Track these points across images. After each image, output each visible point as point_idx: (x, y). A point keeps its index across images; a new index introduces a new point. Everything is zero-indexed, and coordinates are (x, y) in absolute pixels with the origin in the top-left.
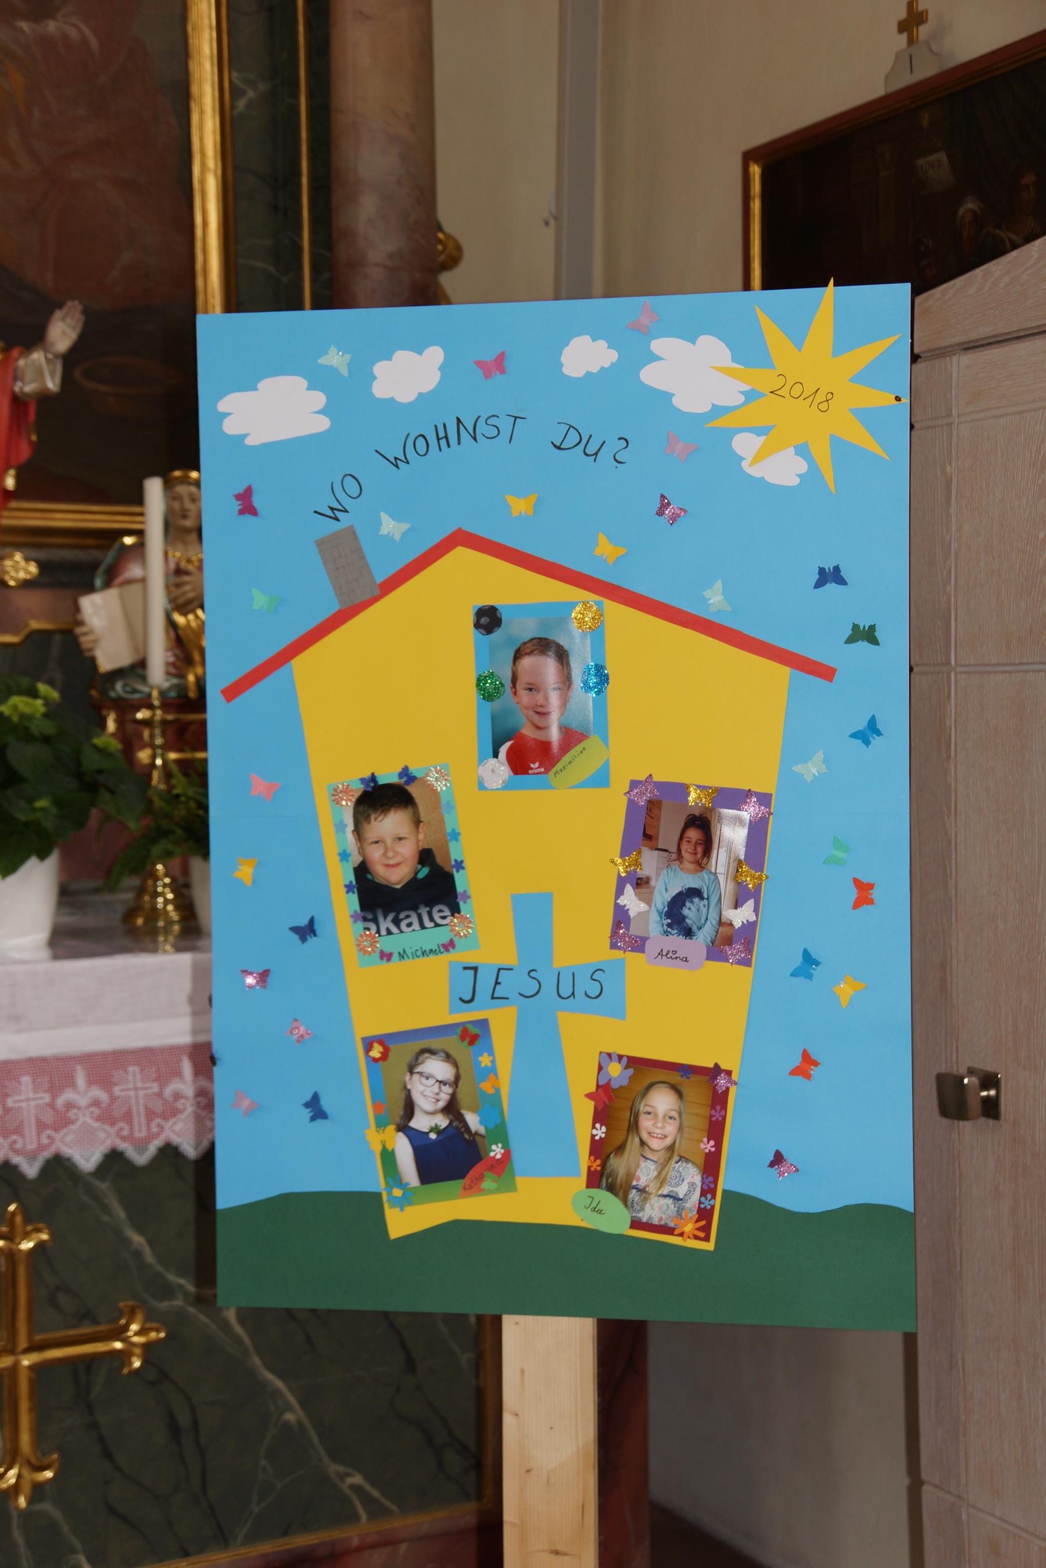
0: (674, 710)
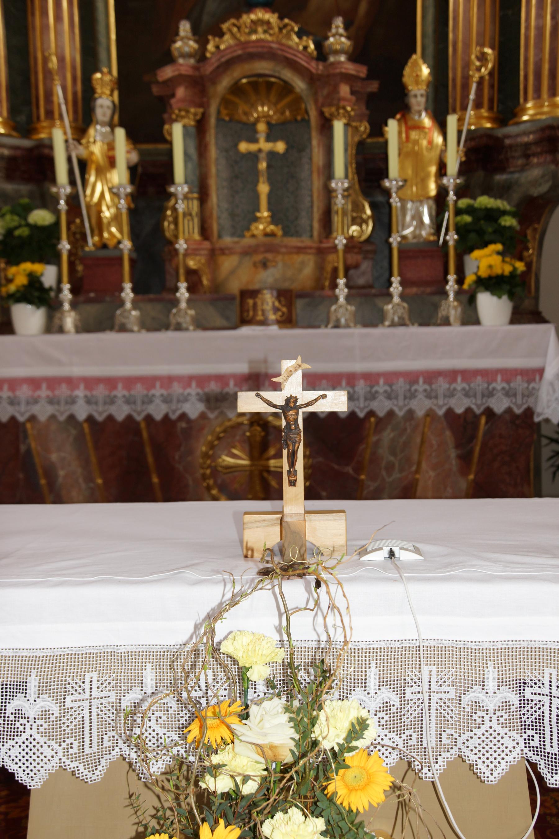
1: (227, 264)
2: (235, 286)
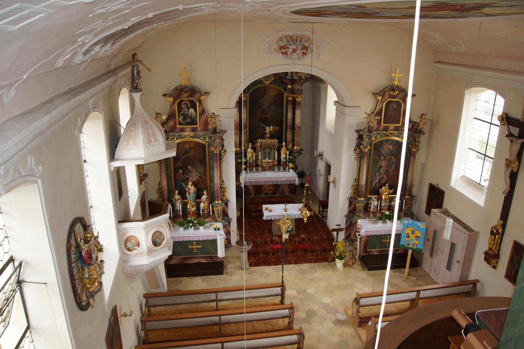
0: (417, 233)
1: (263, 164)
2: (264, 166)
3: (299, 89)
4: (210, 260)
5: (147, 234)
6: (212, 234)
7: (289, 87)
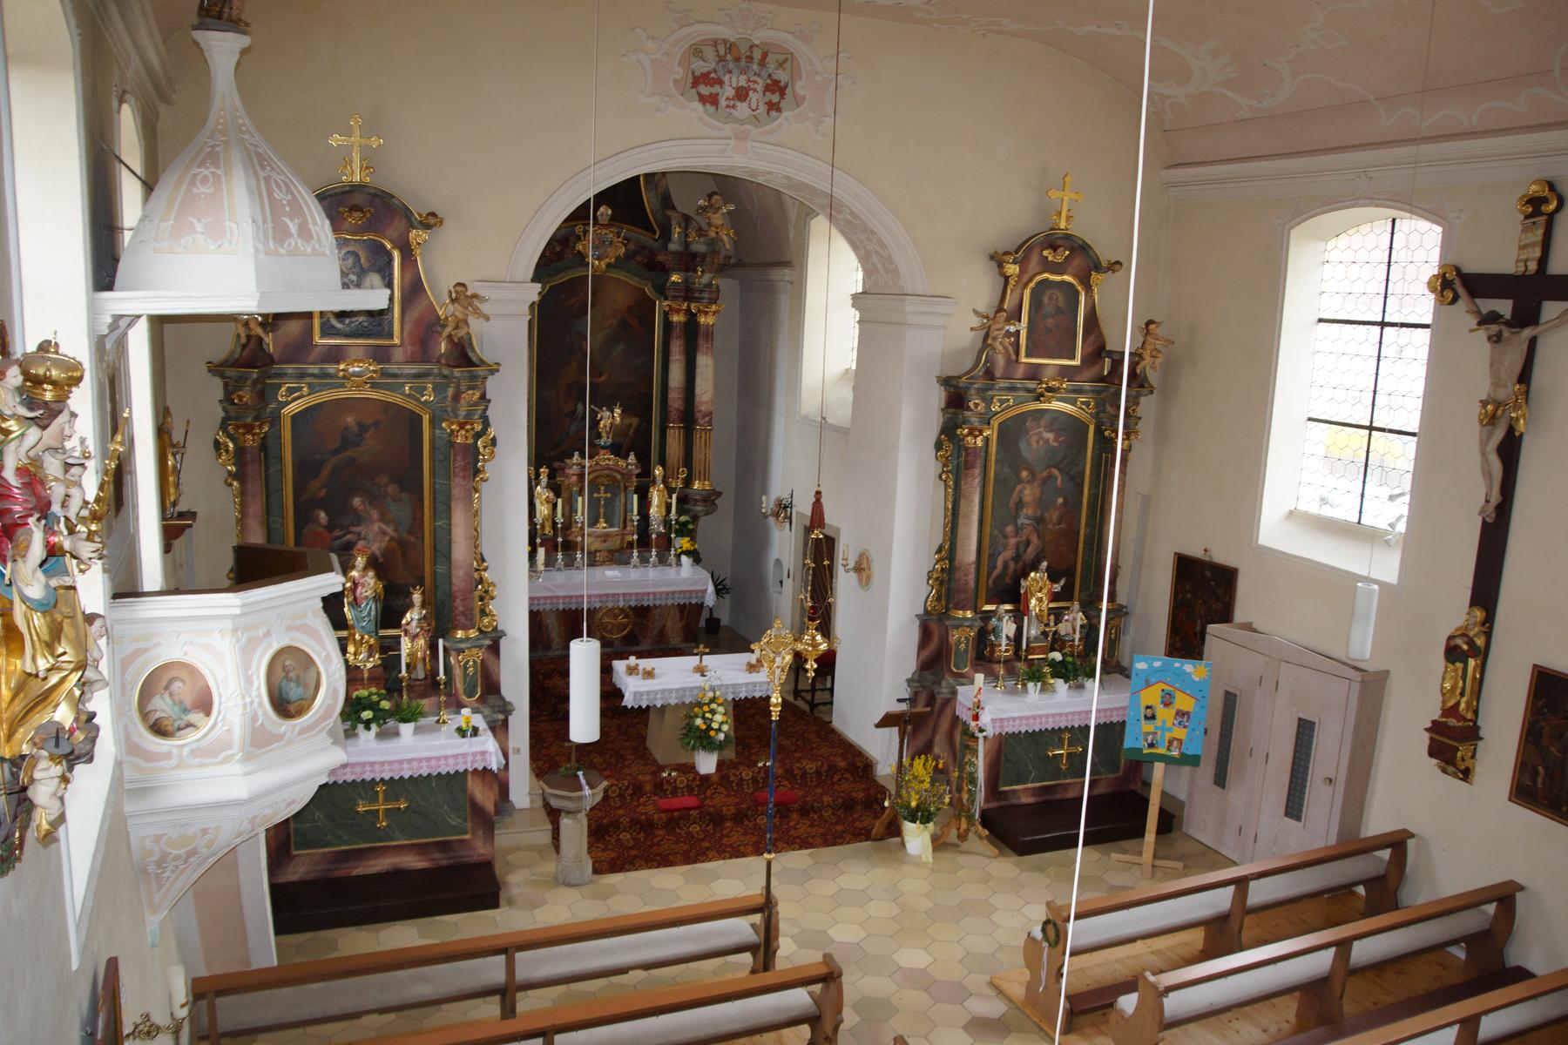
0: (1183, 702)
3: (709, 285)
4: (441, 859)
5: (246, 652)
6: (450, 752)
7: (675, 278)
